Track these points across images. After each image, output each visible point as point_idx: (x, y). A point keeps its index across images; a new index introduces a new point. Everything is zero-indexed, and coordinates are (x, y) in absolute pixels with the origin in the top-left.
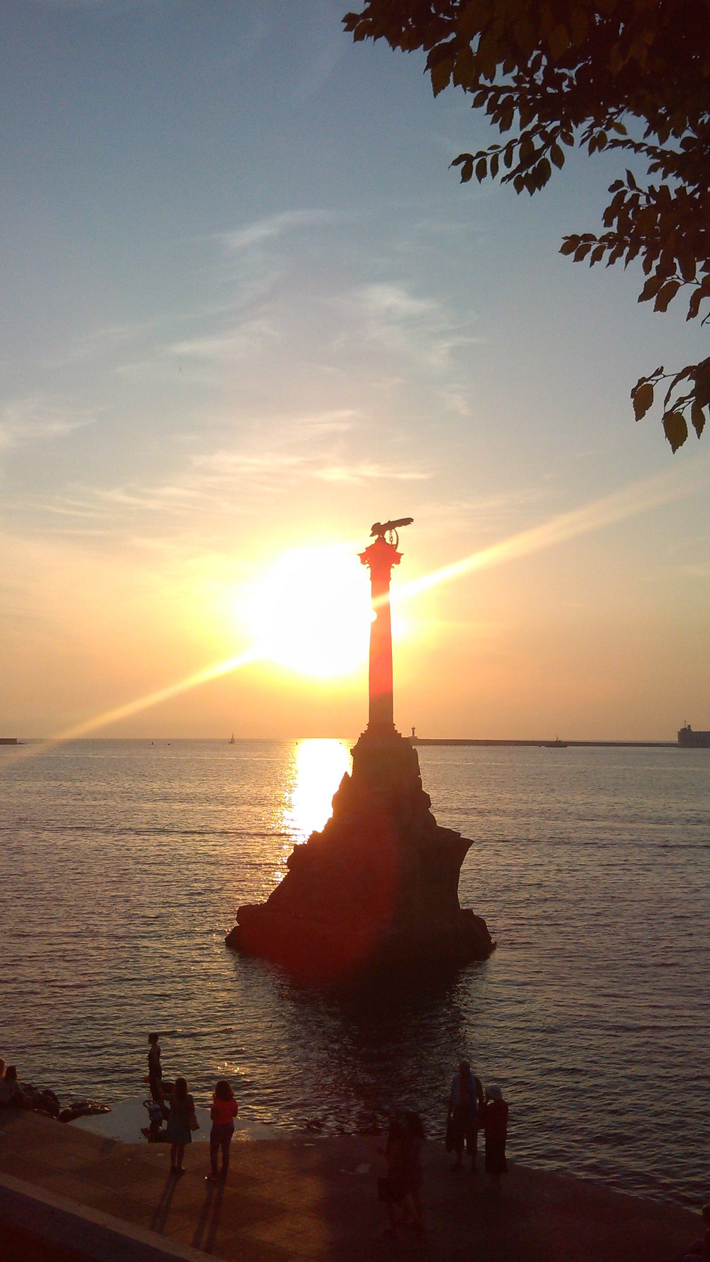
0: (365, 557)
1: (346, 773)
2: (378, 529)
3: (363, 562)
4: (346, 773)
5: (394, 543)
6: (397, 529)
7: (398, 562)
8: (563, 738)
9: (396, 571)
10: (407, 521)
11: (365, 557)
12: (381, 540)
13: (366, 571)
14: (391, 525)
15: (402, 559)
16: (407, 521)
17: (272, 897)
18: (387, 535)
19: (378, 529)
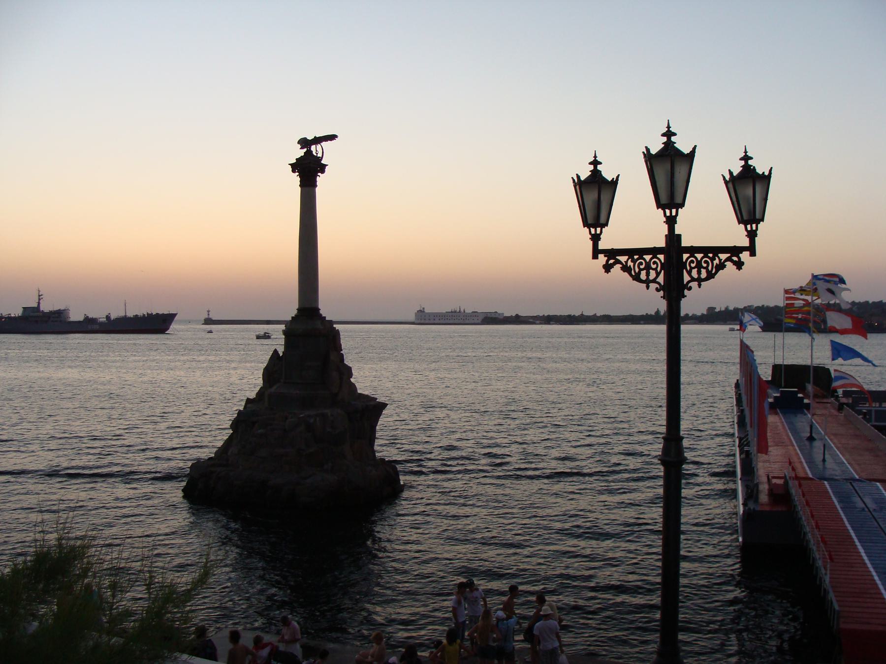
0: (295, 167)
1: (276, 352)
2: (305, 143)
3: (294, 171)
4: (276, 352)
5: (320, 155)
6: (324, 144)
7: (323, 172)
8: (523, 313)
9: (321, 179)
10: (332, 137)
11: (295, 167)
12: (309, 152)
13: (295, 179)
14: (318, 140)
15: (327, 168)
16: (332, 137)
17: (216, 453)
18: (313, 148)
19: (305, 143)
